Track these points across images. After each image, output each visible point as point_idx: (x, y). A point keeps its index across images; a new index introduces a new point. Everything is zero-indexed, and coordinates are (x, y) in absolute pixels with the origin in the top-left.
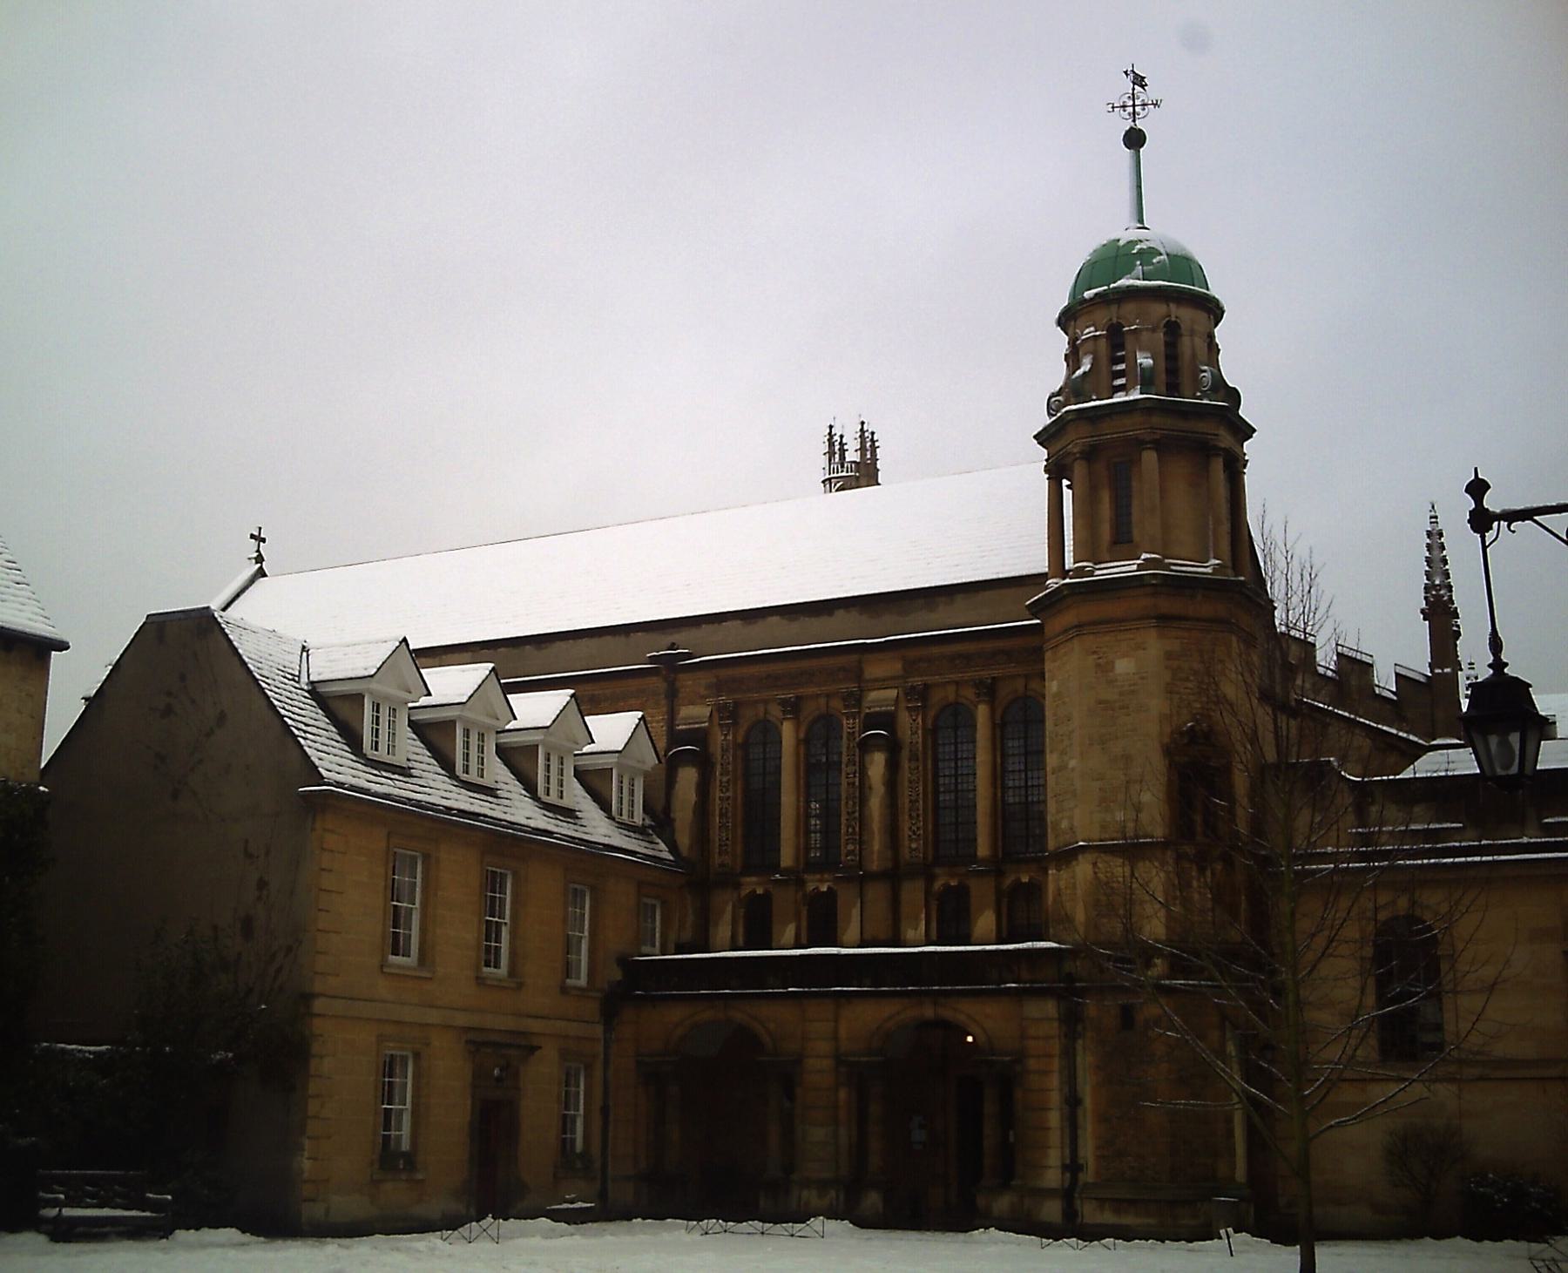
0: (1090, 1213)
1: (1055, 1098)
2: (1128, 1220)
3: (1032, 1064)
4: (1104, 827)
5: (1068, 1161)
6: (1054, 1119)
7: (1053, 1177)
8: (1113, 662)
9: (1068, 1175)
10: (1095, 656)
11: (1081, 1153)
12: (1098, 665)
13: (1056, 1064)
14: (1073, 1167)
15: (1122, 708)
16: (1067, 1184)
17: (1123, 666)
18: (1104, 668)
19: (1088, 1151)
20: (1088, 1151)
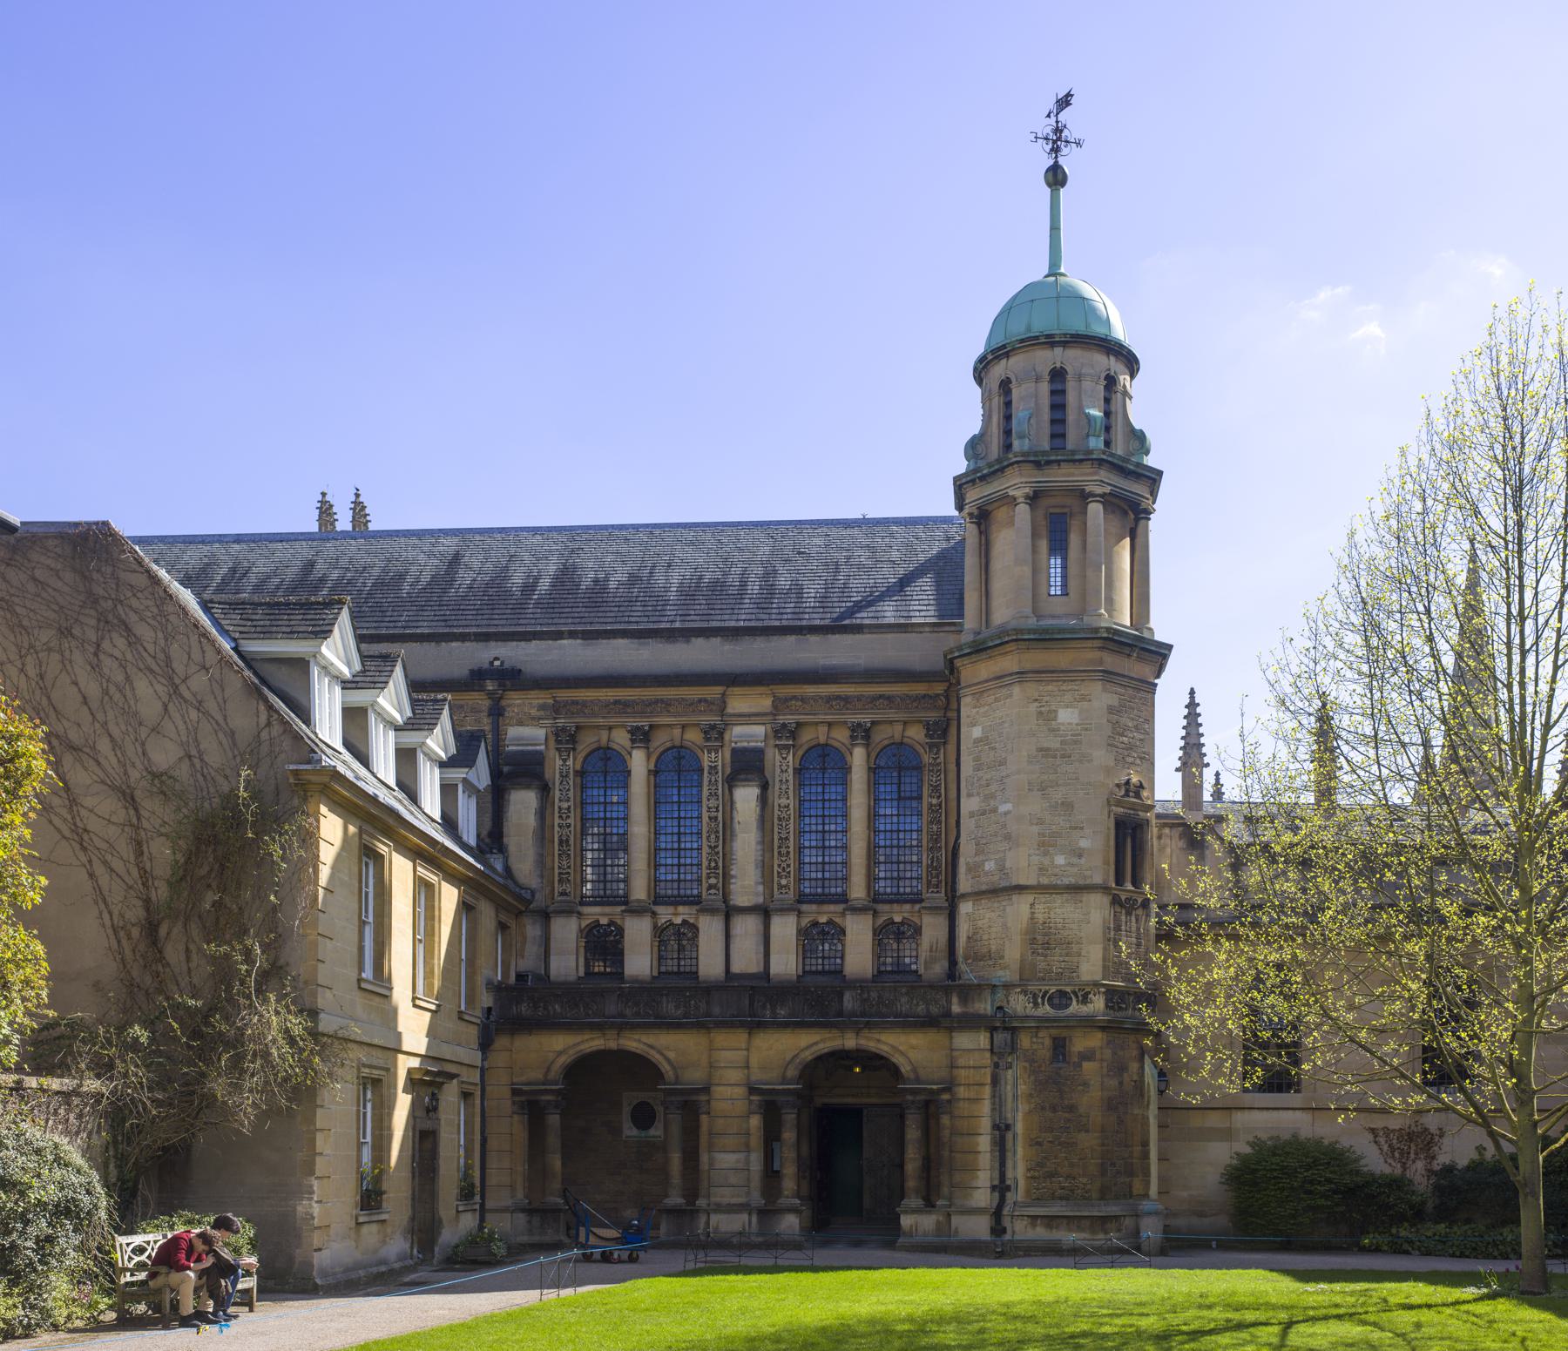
0: (1020, 1230)
1: (985, 1124)
2: (1070, 1237)
3: (962, 1092)
4: (1042, 870)
5: (996, 1182)
6: (984, 1143)
7: (982, 1197)
8: (1056, 712)
9: (997, 1194)
10: (1036, 704)
11: (1009, 1174)
12: (1041, 713)
13: (987, 1090)
14: (1001, 1188)
15: (1063, 756)
16: (995, 1204)
17: (1067, 717)
18: (1047, 716)
19: (1018, 1171)
20: (1018, 1171)
